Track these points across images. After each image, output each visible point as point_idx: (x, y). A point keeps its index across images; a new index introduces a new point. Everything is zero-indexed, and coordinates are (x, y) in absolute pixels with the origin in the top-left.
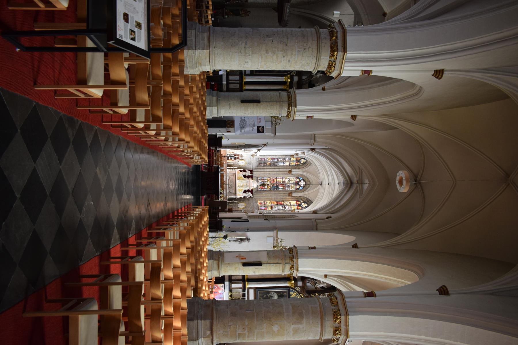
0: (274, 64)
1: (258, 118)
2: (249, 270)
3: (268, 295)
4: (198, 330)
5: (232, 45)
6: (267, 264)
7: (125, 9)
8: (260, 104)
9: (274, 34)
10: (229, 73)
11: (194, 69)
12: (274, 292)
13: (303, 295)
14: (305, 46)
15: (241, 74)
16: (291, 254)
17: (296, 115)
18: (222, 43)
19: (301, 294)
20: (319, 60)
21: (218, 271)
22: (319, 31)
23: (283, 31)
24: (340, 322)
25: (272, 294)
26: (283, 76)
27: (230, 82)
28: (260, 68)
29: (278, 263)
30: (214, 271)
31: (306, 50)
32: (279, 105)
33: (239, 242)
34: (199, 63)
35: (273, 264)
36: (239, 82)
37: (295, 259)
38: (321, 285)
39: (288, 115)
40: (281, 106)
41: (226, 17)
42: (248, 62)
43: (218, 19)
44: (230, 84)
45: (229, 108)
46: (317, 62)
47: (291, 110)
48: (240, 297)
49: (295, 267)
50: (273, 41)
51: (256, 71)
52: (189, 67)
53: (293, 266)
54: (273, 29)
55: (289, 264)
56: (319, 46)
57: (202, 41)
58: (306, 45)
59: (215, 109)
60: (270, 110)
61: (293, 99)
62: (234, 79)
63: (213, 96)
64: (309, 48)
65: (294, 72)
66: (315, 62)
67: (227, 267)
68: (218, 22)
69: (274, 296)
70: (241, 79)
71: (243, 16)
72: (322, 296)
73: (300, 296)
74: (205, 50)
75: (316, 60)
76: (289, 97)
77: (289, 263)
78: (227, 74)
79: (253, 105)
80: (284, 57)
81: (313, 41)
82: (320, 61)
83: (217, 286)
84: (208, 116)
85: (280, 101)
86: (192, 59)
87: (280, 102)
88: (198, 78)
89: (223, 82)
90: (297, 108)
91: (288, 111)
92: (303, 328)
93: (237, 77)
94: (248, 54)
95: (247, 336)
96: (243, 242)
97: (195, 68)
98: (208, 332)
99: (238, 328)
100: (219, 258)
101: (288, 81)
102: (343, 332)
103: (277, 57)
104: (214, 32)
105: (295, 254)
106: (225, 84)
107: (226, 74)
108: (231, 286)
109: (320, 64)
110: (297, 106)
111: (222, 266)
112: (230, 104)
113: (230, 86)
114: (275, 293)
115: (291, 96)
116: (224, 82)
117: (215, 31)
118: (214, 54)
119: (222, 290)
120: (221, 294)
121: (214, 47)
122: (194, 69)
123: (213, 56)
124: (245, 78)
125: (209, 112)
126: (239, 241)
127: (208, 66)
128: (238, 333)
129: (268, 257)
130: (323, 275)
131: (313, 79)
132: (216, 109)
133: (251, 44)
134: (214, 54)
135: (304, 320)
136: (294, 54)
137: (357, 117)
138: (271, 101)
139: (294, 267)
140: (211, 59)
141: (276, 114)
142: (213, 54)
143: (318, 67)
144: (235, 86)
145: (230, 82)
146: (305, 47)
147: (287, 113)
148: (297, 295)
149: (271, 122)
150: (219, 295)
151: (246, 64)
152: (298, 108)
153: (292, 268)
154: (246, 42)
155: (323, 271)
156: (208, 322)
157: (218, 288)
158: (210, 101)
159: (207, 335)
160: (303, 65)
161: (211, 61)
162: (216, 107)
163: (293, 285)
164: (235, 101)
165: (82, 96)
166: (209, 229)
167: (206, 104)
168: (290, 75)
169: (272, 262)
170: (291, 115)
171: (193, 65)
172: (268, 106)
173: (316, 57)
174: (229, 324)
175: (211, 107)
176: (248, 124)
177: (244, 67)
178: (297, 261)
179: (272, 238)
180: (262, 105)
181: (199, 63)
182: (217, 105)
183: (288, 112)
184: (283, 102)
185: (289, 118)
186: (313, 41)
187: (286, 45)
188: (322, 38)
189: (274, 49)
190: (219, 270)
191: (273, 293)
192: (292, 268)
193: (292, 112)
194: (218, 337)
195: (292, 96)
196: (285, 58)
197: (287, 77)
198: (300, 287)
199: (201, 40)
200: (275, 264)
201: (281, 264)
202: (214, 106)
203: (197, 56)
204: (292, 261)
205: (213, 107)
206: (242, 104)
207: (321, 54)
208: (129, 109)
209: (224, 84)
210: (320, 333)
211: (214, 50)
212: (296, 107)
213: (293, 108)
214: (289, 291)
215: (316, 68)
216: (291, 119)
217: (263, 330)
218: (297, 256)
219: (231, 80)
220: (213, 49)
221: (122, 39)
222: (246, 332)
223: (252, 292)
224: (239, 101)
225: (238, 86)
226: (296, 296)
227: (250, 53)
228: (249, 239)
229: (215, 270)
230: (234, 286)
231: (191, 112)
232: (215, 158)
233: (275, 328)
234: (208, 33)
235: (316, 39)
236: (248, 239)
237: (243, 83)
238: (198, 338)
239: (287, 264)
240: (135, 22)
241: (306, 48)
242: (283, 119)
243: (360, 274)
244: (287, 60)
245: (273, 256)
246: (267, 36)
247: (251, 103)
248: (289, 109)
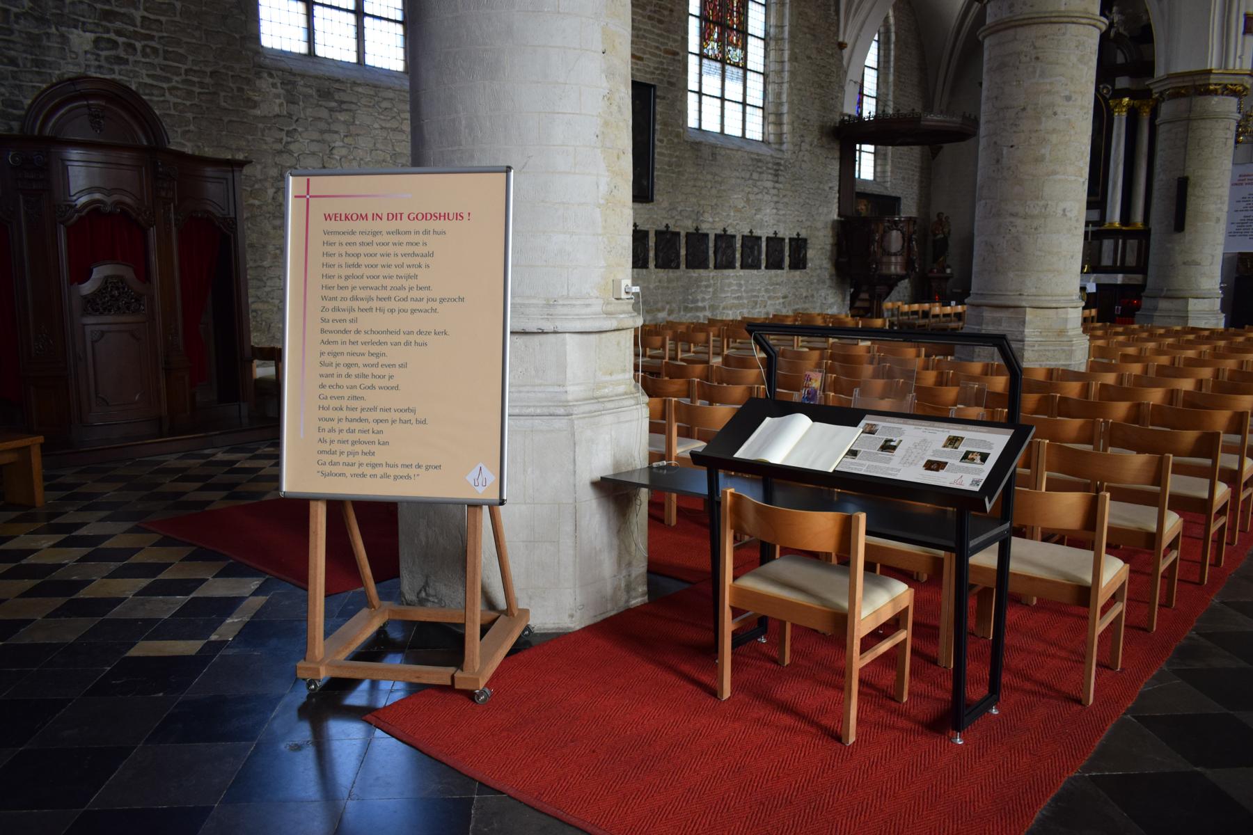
0: (1072, 138)
1: (1236, 184)
5: (1018, 251)
7: (916, 464)
8: (1191, 178)
9: (995, 143)
10: (1092, 263)
11: (1074, 348)
14: (1028, 59)
15: (1095, 235)
17: (1237, 67)
18: (1011, 275)
20: (1068, 17)
22: (992, 27)
23: (988, 122)
26: (1113, 119)
27: (1118, 264)
28: (1081, 176)
31: (1040, 55)
32: (1199, 121)
34: (1058, 335)
36: (1120, 241)
39: (1234, 93)
40: (1204, 117)
41: (948, 271)
42: (1064, 210)
43: (955, 290)
45: (1199, 264)
46: (1074, 20)
47: (1220, 84)
50: (1012, 146)
51: (1091, 192)
52: (1066, 360)
54: (981, 148)
56: (1030, 21)
57: (1004, 324)
58: (1026, 56)
59: (1195, 305)
60: (1213, 148)
61: (1184, 82)
62: (1112, 254)
63: (1155, 309)
64: (1035, 48)
65: (1103, 88)
66: (1074, 25)
68: (959, 291)
70: (1113, 233)
71: (949, 231)
74: (1027, 319)
75: (1070, 25)
76: (1177, 94)
78: (1094, 272)
79: (1193, 198)
80: (1055, 114)
81: (1018, 37)
82: (1072, 12)
84: (1217, 324)
85: (1188, 121)
86: (1049, 351)
87: (1189, 119)
88: (1100, 342)
89: (1119, 282)
90: (1213, 67)
91: (1222, 94)
93: (1108, 244)
94: (1043, 210)
97: (1072, 345)
101: (1128, 105)
103: (1054, 131)
104: (982, 294)
106: (1123, 278)
109: (1080, 12)
110: (1209, 68)
112: (1184, 263)
113: (1130, 265)
115: (1173, 88)
116: (1119, 279)
117: (980, 292)
118: (1039, 296)
121: (1020, 295)
122: (1074, 348)
123: (1043, 298)
124: (1111, 224)
127: (1067, 313)
131: (1125, 33)
132: (1196, 301)
133: (1015, 202)
134: (1039, 296)
136: (1048, 87)
138: (1186, 145)
140: (1049, 305)
141: (1229, 129)
142: (1038, 298)
143: (1091, 16)
145: (1118, 264)
146: (1031, 59)
147: (1227, 95)
151: (1068, 214)
152: (1213, 63)
154: (1012, 215)
158: (1169, 316)
160: (1081, 60)
161: (1054, 305)
162: (1191, 301)
164: (1177, 248)
165: (1119, 607)
167: (1179, 328)
168: (1110, 98)
170: (1235, 85)
171: (1064, 351)
172: (1199, 154)
173: (1062, 25)
175: (1190, 315)
177: (1077, 221)
180: (1194, 170)
181: (1058, 335)
182: (1186, 299)
183: (1225, 92)
184: (1190, 112)
185: (1245, 89)
186: (1015, 39)
187: (1024, 109)
188: (1011, 15)
189: (1033, 141)
193: (1227, 80)
195: (1174, 86)
196: (1059, 110)
197: (1116, 107)
199: (1001, 325)
203: (1039, 339)
206: (1187, 227)
207: (1052, 12)
208: (1169, 509)
209: (1123, 280)
211: (1028, 295)
212: (1211, 70)
215: (1092, 22)
216: (1248, 82)
219: (1115, 261)
220: (1024, 297)
221: (983, 481)
224: (1177, 236)
225: (1133, 243)
227: (1041, 203)
231: (1199, 362)
234: (985, 308)
235: (1011, 32)
237: (1124, 228)
240: (945, 449)
241: (1034, 56)
242: (1248, 109)
244: (1066, 103)
246: (998, 161)
247: (1188, 203)
248: (1215, 92)
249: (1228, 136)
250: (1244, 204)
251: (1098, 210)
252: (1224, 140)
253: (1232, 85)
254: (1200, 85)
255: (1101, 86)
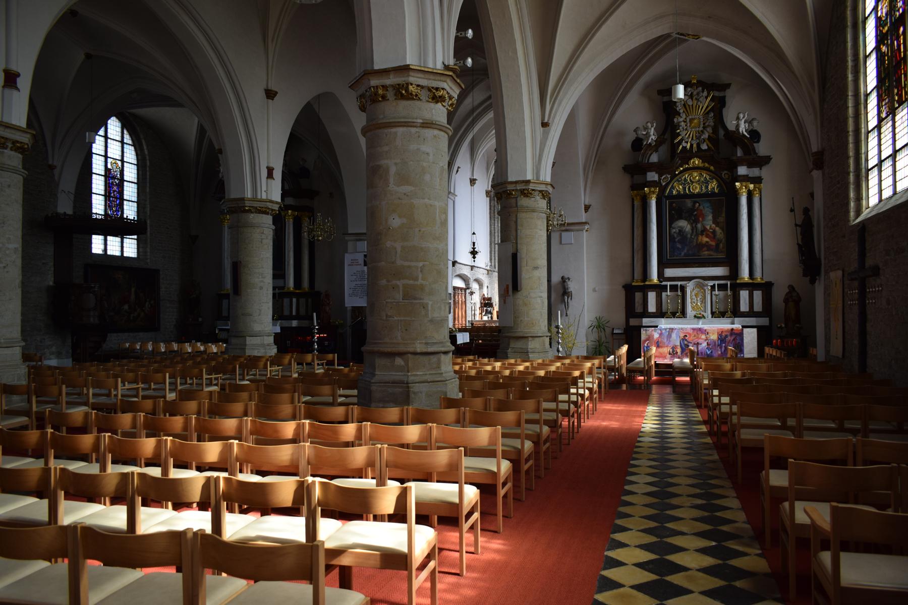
2: (529, 278)
3: (677, 240)
4: (389, 383)
6: (517, 243)
10: (278, 314)
12: (670, 227)
13: (678, 168)
15: (279, 295)
16: (502, 197)
19: (677, 173)
21: (530, 339)
24: (383, 86)
25: (674, 230)
29: (516, 222)
30: (529, 347)
33: (568, 298)
35: (519, 231)
37: (508, 189)
38: (652, 133)
41: (200, 319)
47: (252, 207)
48: (678, 295)
49: (524, 188)
51: (275, 267)
53: (521, 192)
55: (518, 199)
59: (251, 341)
67: (521, 320)
69: (680, 227)
72: (682, 130)
73: (679, 174)
77: (517, 200)
83: (645, 341)
92: (396, 164)
93: (286, 301)
95: (411, 282)
96: (569, 290)
98: (399, 361)
99: (393, 301)
100: (506, 337)
102: (403, 79)
105: (501, 188)
107: (280, 321)
108: (652, 313)
111: (519, 330)
112: (243, 315)
114: (673, 226)
116: (295, 323)
119: (652, 331)
120: (661, 334)
124: (289, 288)
125: (256, 351)
126: (566, 297)
128: (403, 299)
129: (506, 242)
130: (544, 131)
135: (383, 162)
137: (270, 88)
138: (238, 242)
139: (524, 189)
141: (263, 233)
148: (679, 181)
149: (357, 242)
150: (663, 337)
153: (526, 193)
155: (533, 131)
156: (380, 362)
157: (647, 339)
159: (403, 363)
163: (653, 189)
166: (470, 355)
169: (514, 234)
170: (262, 207)
174: (385, 318)
176: (360, 283)
178: (512, 183)
179: (564, 234)
182: (245, 337)
190: (528, 337)
191: (673, 229)
192: (525, 193)
194: (409, 342)
198: (660, 176)
200: (519, 228)
201: (518, 215)
202: (246, 340)
204: (512, 194)
205: (247, 343)
210: (410, 128)
213: (247, 203)
214: (671, 196)
217: (399, 250)
218: (502, 184)
222: (400, 283)
223: (669, 272)
226: (680, 183)
228: (563, 278)
229: (527, 345)
230: (652, 308)
232: (480, 341)
233: (395, 222)
236: (564, 280)
237: (297, 291)
238: (404, 383)
239: (519, 204)
243: (526, 55)
245: (505, 231)
248: (250, 211)
249: (263, 237)
250: (355, 277)
252: (260, 240)
253: (260, 207)
254: (241, 207)
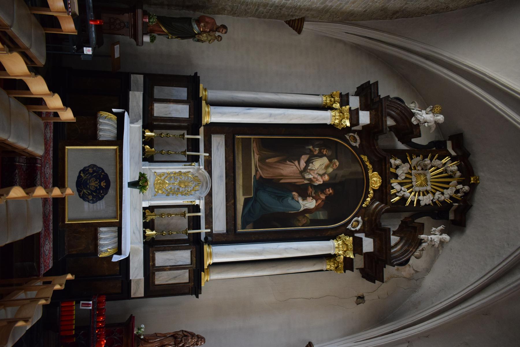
41: (147, 39)
43: (117, 48)
44: (156, 273)
68: (117, 55)
71: (203, 41)
106: (142, 279)
113: (156, 277)
124: (210, 255)
144: (175, 278)
225: (184, 277)
251: (225, 232)
255: (360, 219)
